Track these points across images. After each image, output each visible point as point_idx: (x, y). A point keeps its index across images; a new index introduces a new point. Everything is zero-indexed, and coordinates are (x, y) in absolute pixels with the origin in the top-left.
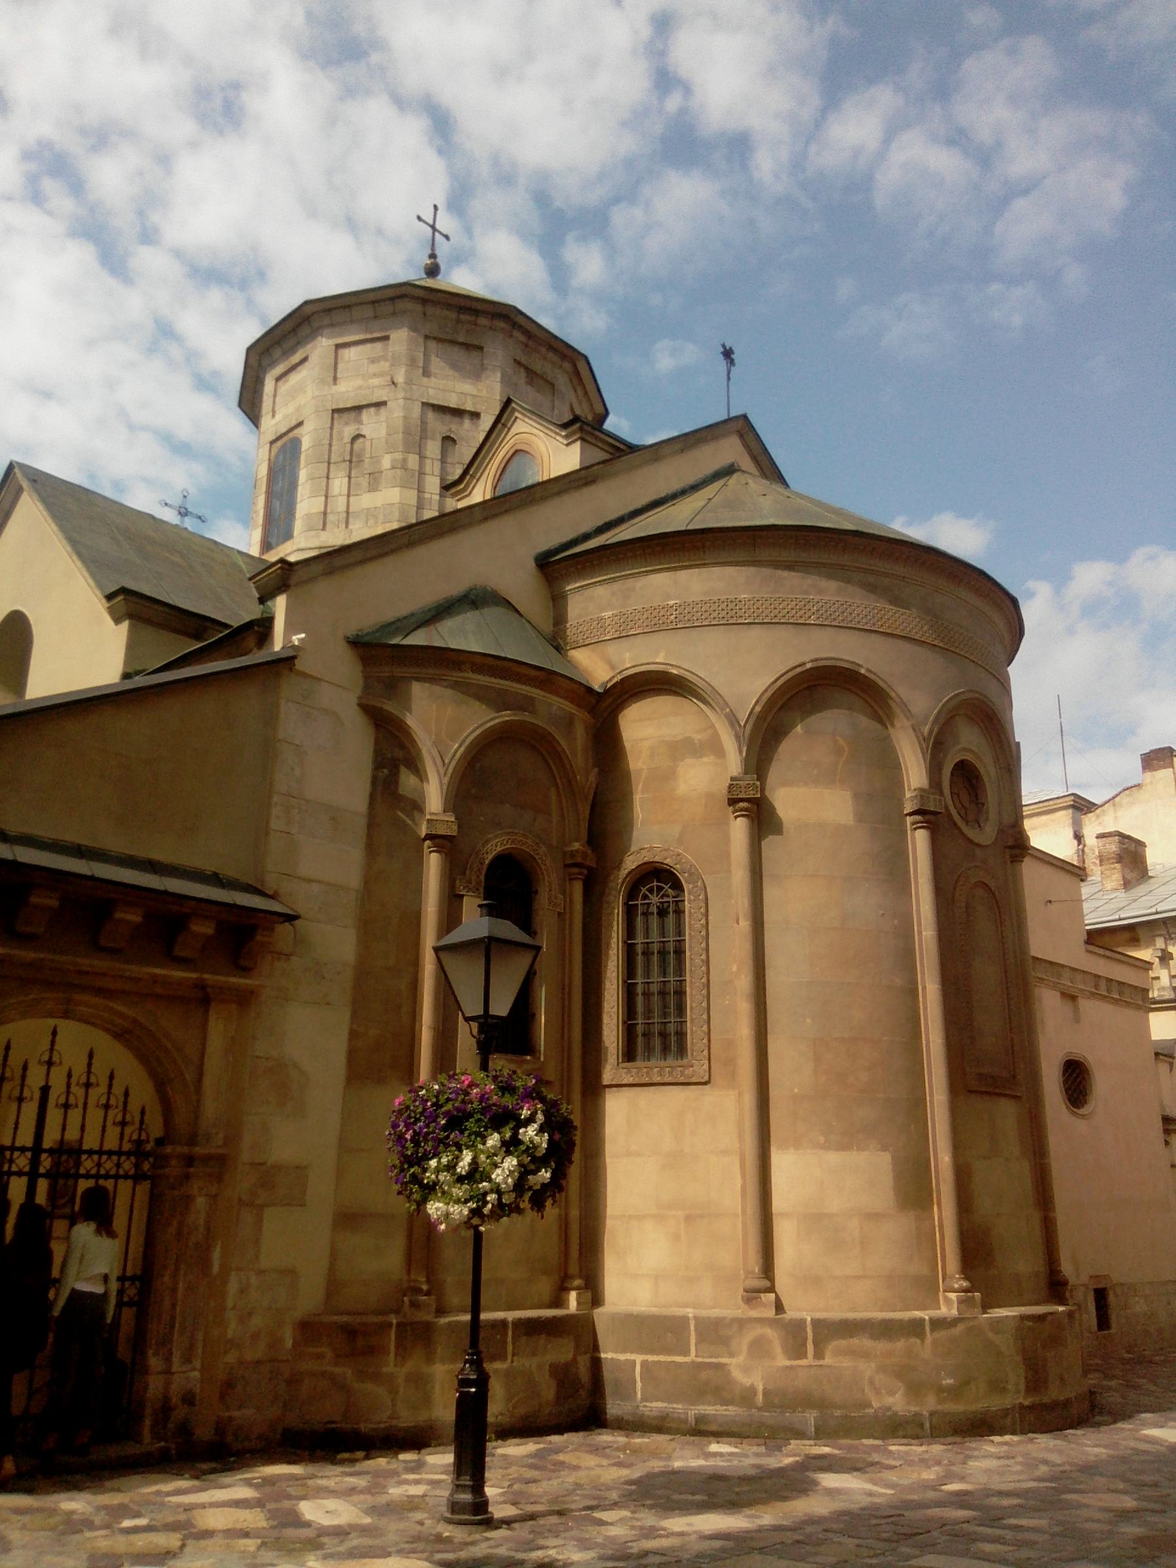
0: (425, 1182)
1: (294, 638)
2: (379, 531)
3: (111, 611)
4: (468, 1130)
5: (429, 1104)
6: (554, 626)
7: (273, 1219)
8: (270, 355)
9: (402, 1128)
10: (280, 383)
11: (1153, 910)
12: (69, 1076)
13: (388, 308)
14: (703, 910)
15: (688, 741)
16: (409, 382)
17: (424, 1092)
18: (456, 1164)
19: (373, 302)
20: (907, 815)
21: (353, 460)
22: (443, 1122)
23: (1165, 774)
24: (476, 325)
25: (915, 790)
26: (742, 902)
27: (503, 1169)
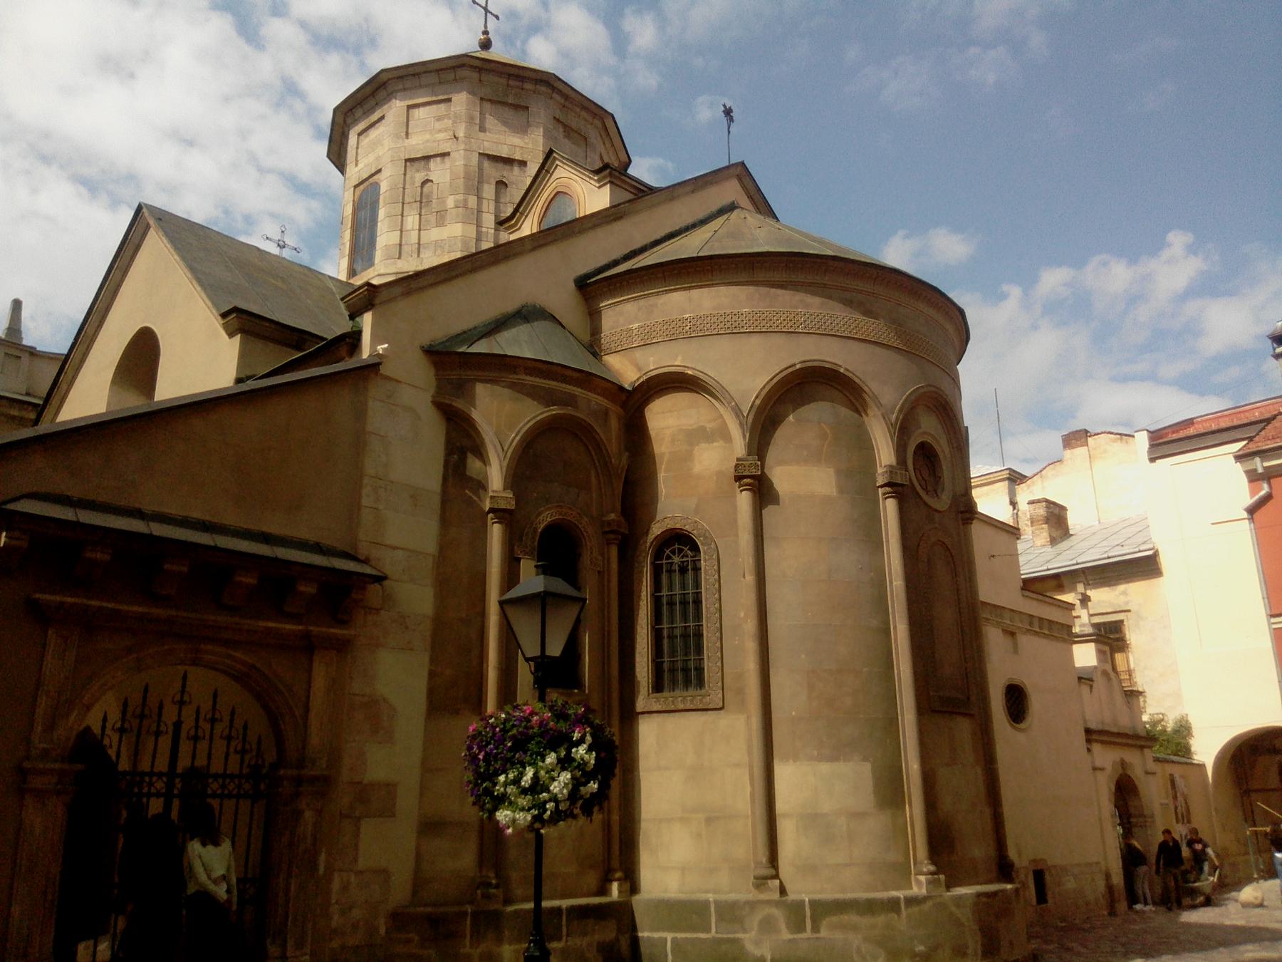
0: (496, 794)
1: (379, 347)
2: (446, 259)
3: (226, 327)
4: (530, 750)
5: (498, 729)
6: (591, 337)
7: (368, 828)
9: (475, 749)
10: (361, 137)
11: (1074, 562)
12: (198, 712)
13: (451, 76)
14: (716, 567)
15: (703, 429)
16: (468, 137)
17: (493, 720)
18: (521, 778)
19: (437, 71)
20: (878, 487)
21: (423, 201)
22: (509, 744)
23: (1081, 451)
24: (522, 89)
25: (885, 466)
26: (748, 560)
27: (559, 782)
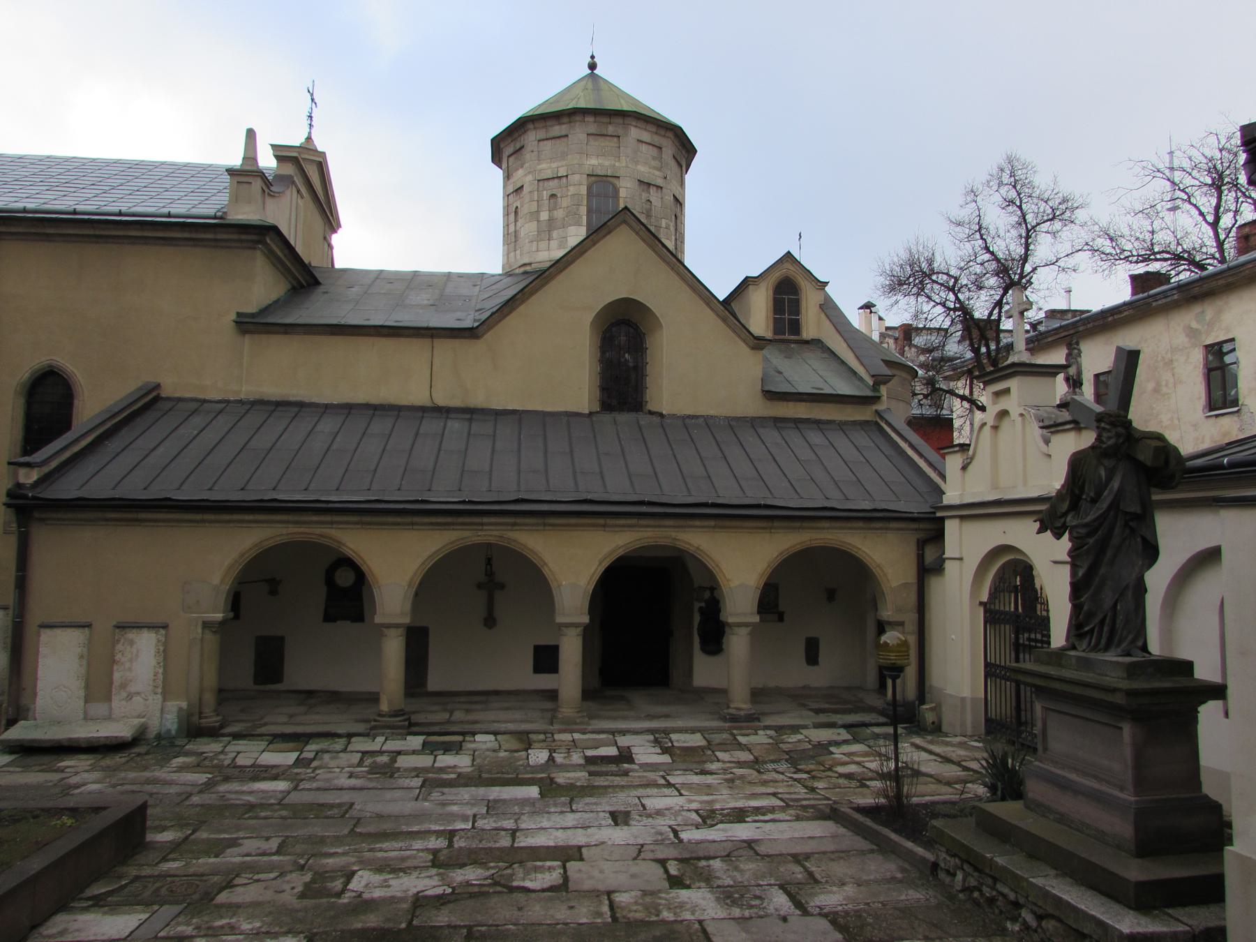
13: (662, 132)
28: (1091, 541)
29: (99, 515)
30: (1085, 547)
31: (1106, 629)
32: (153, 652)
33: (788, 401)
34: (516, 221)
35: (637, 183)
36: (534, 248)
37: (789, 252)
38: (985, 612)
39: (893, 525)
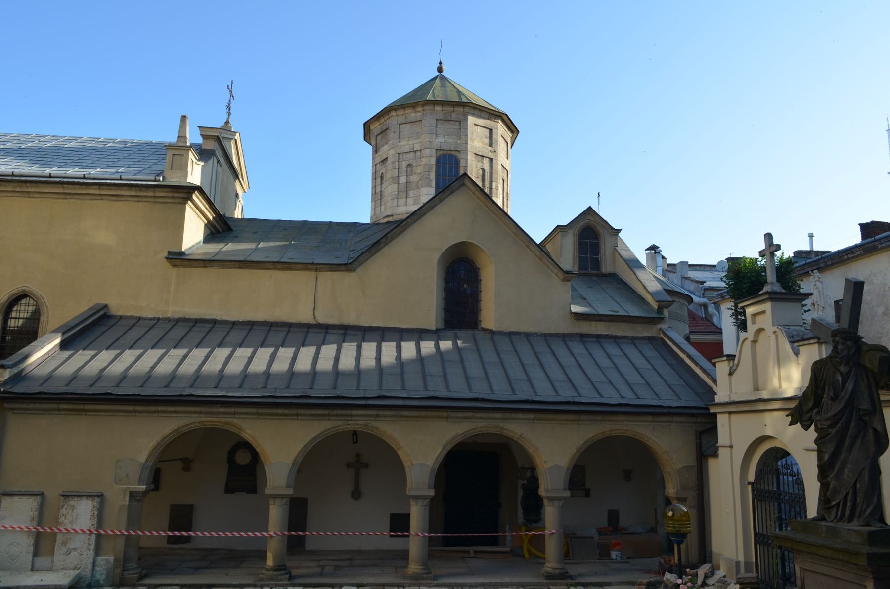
8: (434, 107)
28: (833, 431)
29: (55, 406)
30: (828, 437)
31: (849, 504)
32: (89, 514)
33: (591, 320)
34: (381, 184)
35: (474, 155)
36: (395, 204)
37: (590, 207)
38: (753, 491)
39: (676, 419)
